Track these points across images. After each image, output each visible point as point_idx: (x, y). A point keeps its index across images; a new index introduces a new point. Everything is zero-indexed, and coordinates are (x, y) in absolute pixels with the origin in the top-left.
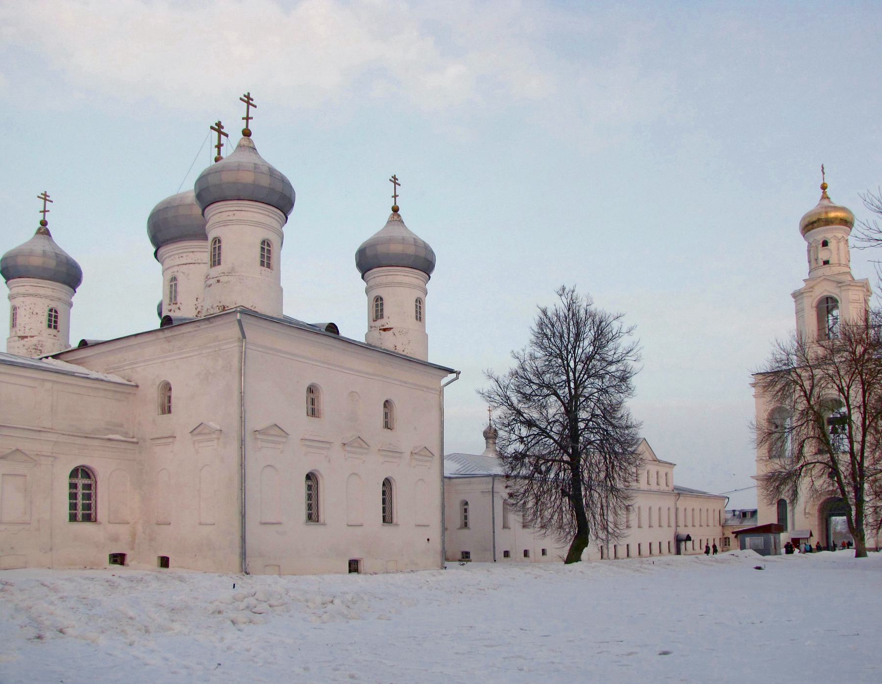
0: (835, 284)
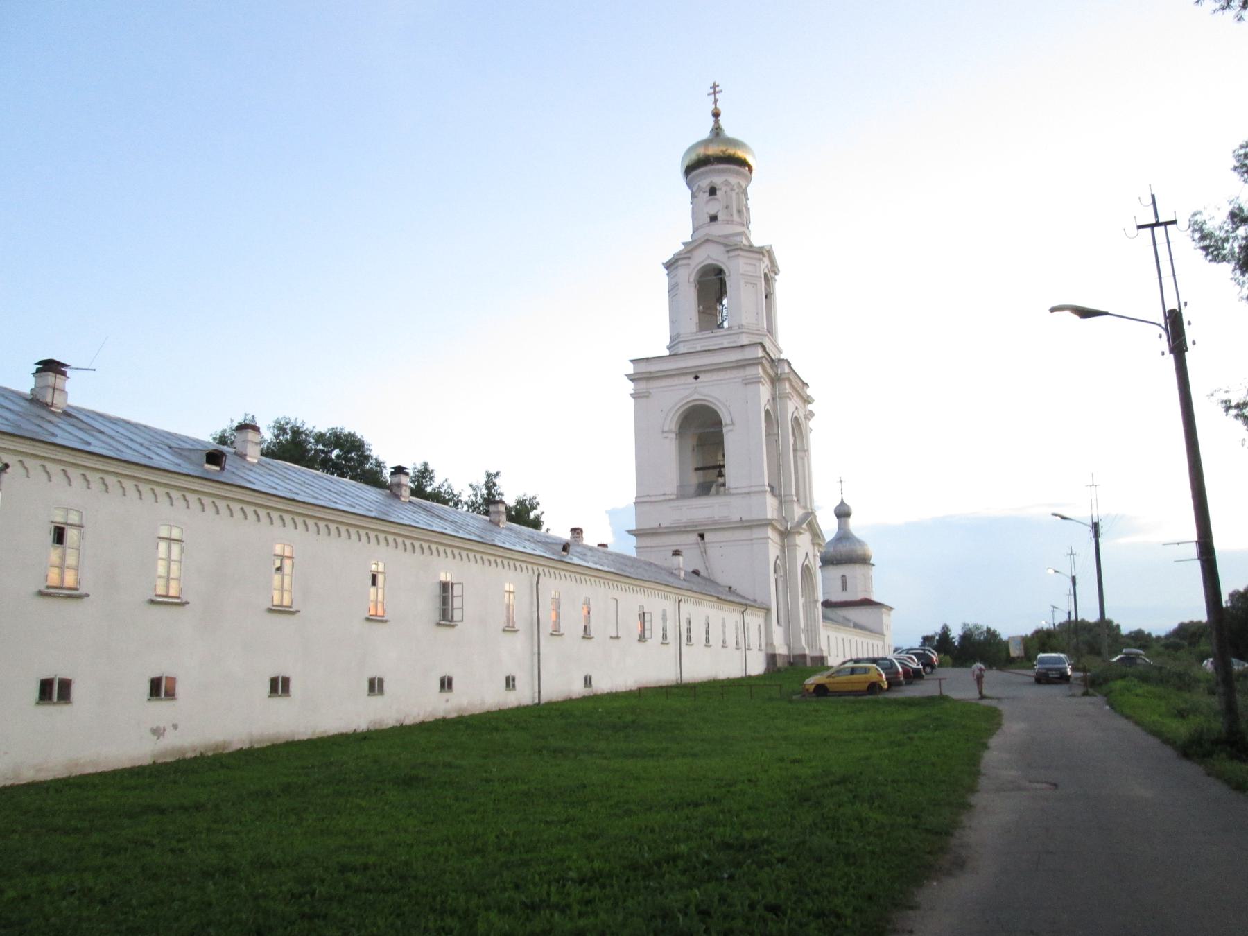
0: (722, 248)
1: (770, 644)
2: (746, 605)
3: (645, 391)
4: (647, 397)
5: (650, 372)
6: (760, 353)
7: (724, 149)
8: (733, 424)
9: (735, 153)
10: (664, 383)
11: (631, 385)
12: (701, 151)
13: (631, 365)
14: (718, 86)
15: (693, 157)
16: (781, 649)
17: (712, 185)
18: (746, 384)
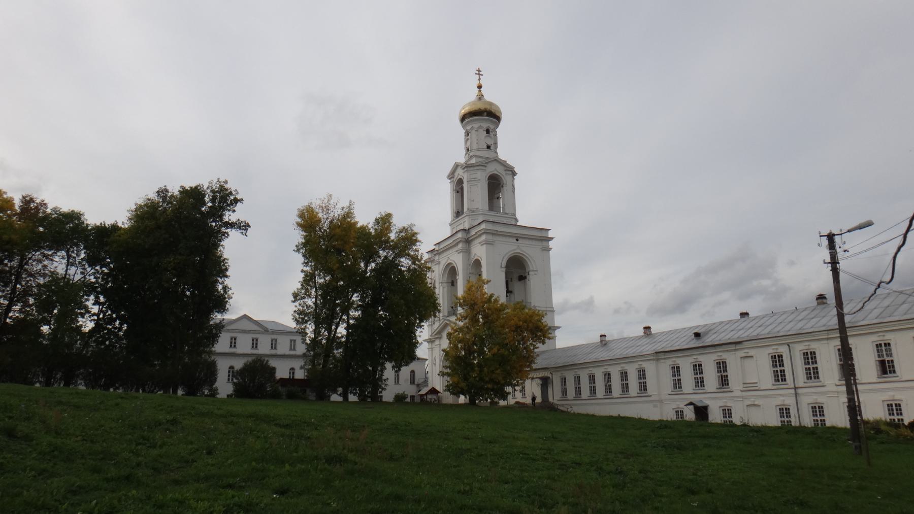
5: (497, 231)
10: (504, 239)
14: (481, 71)
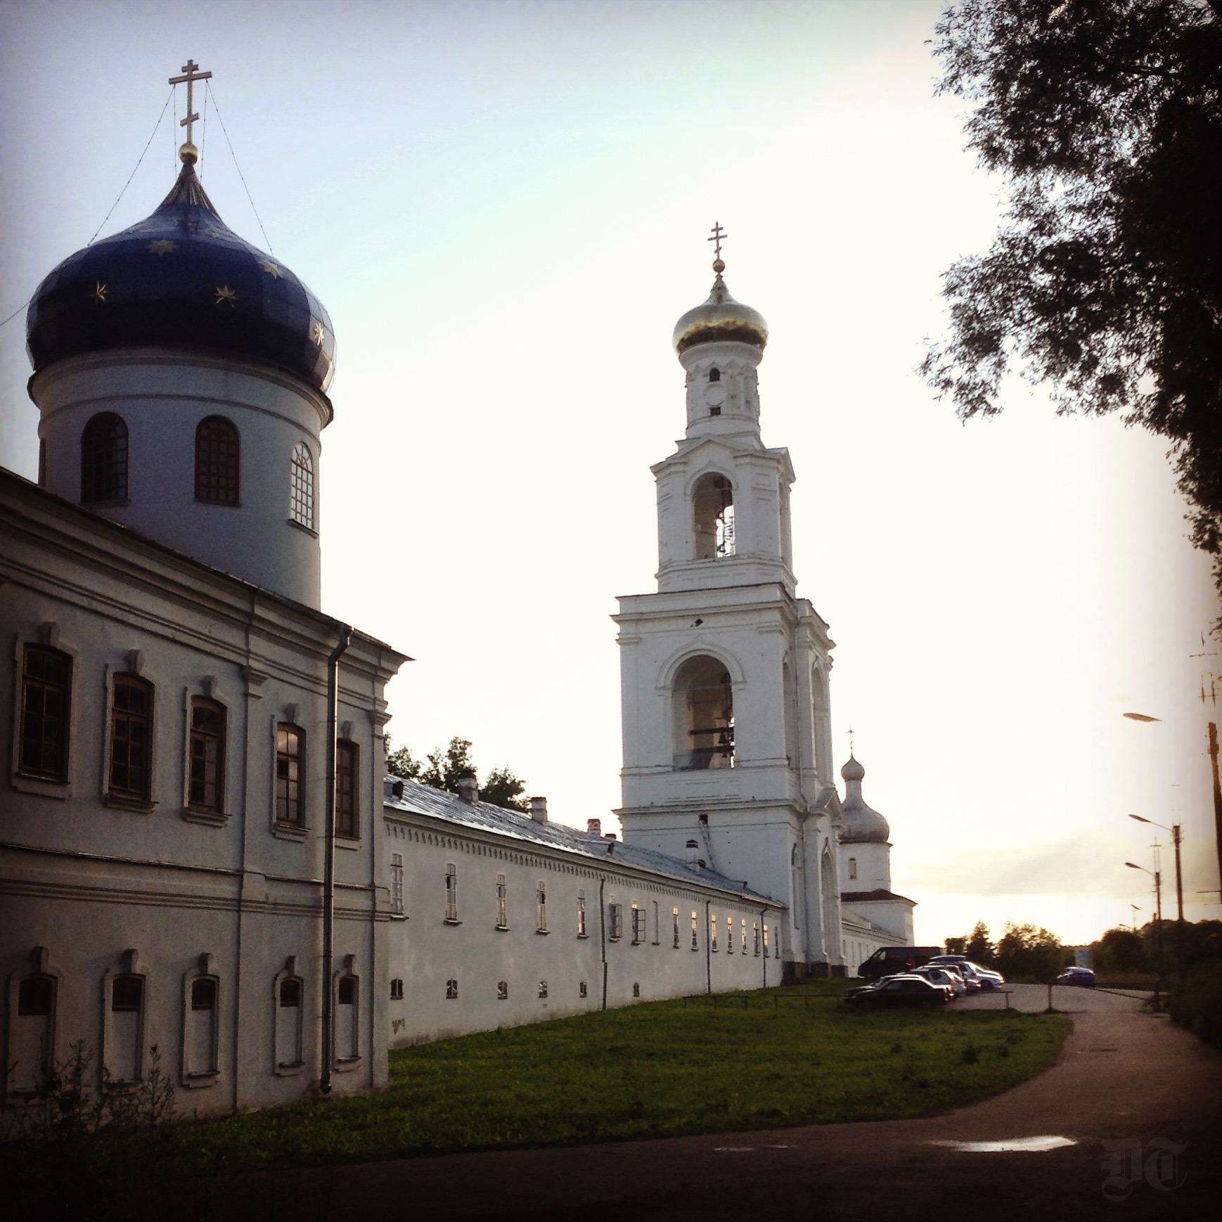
1: (787, 951)
2: (763, 907)
3: (634, 636)
4: (637, 643)
6: (778, 595)
7: (731, 320)
8: (744, 682)
9: (746, 324)
10: (657, 626)
11: (616, 628)
12: (702, 323)
13: (617, 603)
15: (691, 328)
16: (799, 958)
17: (714, 366)
18: (762, 633)
